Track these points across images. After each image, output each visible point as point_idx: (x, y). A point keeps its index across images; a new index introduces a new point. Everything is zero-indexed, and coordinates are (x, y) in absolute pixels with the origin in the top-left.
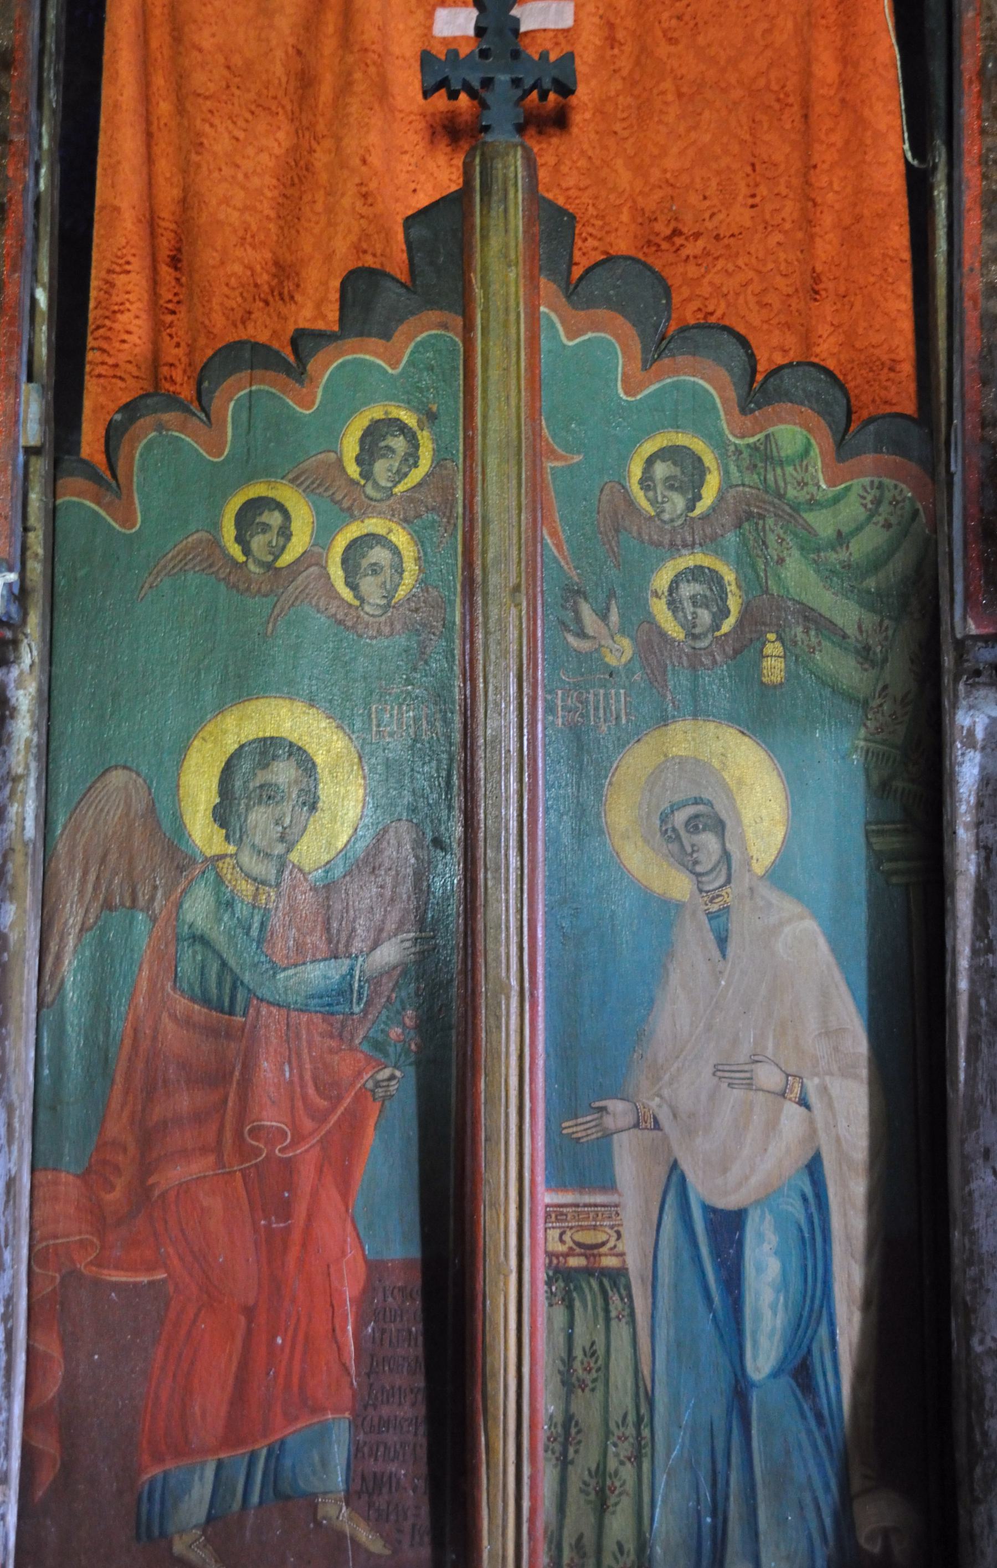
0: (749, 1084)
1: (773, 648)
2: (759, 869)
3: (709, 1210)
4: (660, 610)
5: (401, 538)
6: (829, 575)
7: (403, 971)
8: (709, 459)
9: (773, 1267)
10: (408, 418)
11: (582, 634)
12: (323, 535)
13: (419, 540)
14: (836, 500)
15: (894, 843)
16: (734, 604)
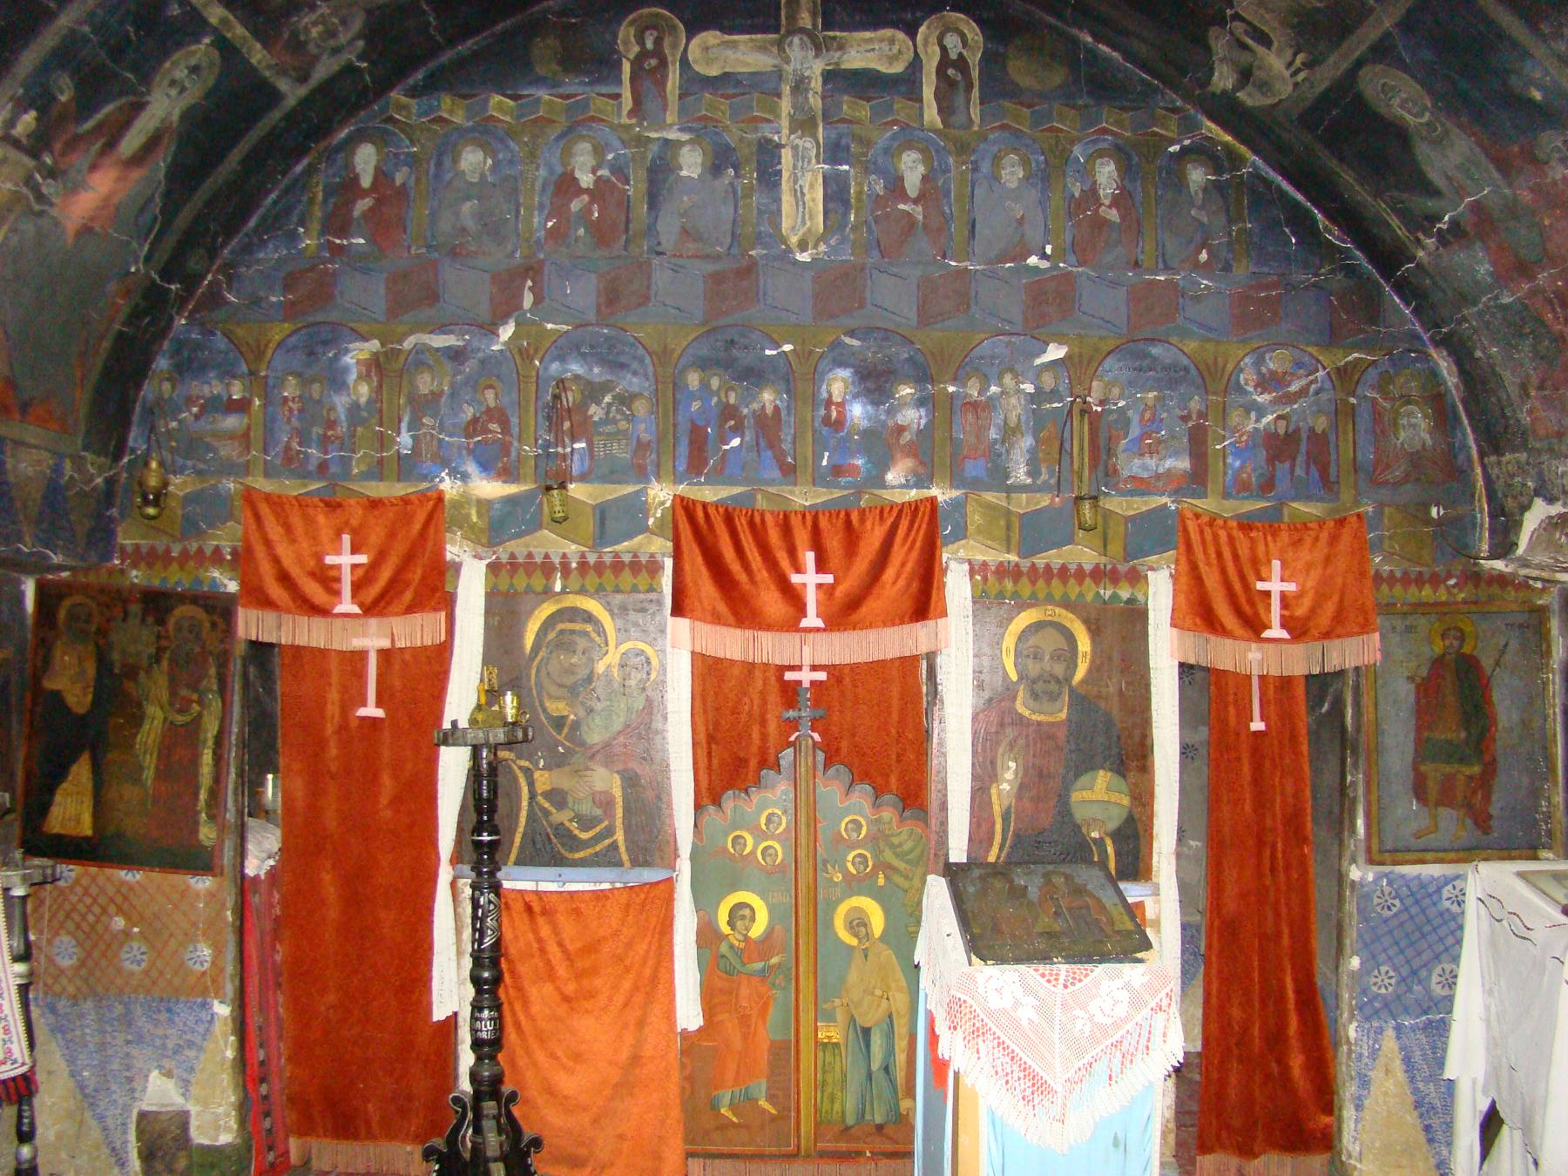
0: (873, 994)
2: (877, 936)
5: (777, 846)
8: (863, 823)
10: (780, 813)
16: (870, 864)
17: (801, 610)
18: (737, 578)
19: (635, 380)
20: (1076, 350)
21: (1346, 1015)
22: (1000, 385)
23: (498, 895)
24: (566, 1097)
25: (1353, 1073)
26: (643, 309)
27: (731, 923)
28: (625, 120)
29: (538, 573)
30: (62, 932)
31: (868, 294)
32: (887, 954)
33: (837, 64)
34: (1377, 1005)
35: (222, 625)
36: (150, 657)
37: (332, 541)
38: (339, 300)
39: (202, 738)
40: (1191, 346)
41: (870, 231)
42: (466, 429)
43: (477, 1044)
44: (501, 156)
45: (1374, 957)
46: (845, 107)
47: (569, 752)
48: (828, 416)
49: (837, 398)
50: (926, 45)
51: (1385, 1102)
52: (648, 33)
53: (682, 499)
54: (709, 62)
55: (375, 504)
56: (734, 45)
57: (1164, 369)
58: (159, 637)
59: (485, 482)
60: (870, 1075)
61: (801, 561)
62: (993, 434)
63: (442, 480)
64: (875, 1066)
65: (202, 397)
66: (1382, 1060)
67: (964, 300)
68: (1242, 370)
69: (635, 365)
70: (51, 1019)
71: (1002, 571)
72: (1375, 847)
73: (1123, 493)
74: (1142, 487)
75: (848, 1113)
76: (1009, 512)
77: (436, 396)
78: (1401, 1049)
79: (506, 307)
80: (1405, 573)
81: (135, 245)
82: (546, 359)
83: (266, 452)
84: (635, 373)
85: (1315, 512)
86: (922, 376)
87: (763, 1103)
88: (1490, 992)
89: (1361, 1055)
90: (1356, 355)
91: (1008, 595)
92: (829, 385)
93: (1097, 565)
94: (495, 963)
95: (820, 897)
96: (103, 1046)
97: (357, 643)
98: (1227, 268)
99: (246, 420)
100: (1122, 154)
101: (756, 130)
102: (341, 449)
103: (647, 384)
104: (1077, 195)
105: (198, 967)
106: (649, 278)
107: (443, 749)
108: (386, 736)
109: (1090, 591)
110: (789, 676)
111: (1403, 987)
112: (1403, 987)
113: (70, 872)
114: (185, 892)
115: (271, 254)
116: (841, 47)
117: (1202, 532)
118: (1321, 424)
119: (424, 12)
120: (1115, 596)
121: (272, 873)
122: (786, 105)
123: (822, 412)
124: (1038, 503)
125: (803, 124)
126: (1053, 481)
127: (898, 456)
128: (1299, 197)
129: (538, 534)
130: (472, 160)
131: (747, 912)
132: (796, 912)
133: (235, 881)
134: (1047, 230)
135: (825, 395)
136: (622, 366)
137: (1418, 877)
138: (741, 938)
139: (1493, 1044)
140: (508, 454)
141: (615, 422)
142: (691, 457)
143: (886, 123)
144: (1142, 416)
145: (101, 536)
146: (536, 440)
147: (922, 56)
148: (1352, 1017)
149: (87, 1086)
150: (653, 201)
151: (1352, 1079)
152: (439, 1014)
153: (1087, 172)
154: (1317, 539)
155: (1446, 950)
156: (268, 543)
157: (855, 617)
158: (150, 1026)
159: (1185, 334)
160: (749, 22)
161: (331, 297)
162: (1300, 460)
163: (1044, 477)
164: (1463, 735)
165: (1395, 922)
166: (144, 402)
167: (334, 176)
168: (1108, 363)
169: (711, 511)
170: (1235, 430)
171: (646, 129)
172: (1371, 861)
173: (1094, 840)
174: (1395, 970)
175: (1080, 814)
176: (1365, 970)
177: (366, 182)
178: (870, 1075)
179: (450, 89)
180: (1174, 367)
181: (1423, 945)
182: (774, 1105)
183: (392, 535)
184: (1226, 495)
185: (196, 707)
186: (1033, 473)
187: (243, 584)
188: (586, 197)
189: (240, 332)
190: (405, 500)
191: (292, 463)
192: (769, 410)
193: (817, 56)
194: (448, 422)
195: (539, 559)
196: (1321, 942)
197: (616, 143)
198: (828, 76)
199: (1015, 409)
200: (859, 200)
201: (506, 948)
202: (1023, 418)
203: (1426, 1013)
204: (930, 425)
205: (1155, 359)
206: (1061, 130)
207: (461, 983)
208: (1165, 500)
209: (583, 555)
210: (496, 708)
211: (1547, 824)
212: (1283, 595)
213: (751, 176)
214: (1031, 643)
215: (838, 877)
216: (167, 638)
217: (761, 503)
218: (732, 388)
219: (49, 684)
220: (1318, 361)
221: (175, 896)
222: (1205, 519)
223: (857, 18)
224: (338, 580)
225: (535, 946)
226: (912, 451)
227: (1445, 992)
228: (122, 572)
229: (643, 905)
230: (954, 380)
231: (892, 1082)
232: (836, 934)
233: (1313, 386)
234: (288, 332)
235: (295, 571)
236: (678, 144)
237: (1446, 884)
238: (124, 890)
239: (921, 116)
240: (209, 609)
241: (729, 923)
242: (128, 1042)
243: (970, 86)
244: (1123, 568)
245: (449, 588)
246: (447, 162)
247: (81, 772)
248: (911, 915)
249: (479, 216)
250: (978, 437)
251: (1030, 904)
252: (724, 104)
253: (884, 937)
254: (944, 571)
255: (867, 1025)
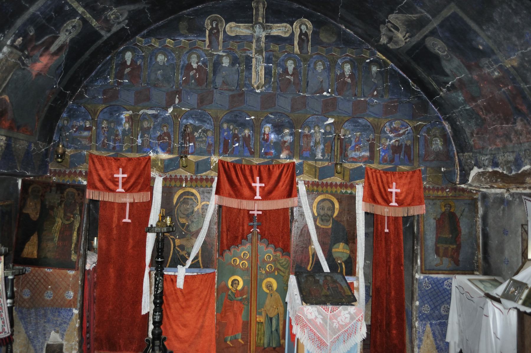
0: (273, 307)
1: (276, 272)
3: (270, 318)
4: (267, 269)
5: (246, 262)
12: (240, 262)
13: (248, 262)
16: (273, 268)
17: (255, 194)
18: (237, 184)
19: (208, 126)
20: (337, 120)
21: (415, 319)
22: (314, 130)
23: (163, 277)
24: (181, 338)
25: (417, 337)
26: (211, 105)
27: (232, 285)
28: (207, 48)
29: (178, 181)
30: (26, 287)
31: (276, 103)
32: (277, 295)
33: (269, 34)
34: (424, 316)
35: (81, 195)
36: (58, 203)
37: (116, 170)
38: (120, 99)
39: (74, 228)
40: (371, 119)
41: (278, 84)
42: (158, 138)
43: (154, 323)
44: (169, 57)
45: (423, 302)
46: (271, 46)
47: (186, 234)
48: (264, 137)
49: (267, 133)
50: (296, 28)
51: (427, 347)
52: (214, 22)
53: (221, 161)
54: (232, 32)
55: (130, 159)
56: (239, 27)
57: (363, 126)
58: (61, 197)
59: (163, 154)
60: (272, 332)
61: (255, 179)
62: (312, 144)
63: (150, 153)
64: (273, 329)
65: (77, 126)
66: (426, 334)
67: (305, 105)
68: (385, 127)
69: (208, 121)
70: (20, 315)
71: (313, 184)
72: (423, 269)
73: (349, 162)
74: (355, 160)
75: (265, 344)
76: (316, 167)
77: (149, 128)
78: (432, 330)
79: (171, 103)
80: (433, 187)
81: (55, 79)
82: (182, 119)
83: (96, 143)
84: (208, 124)
85: (406, 168)
86: (291, 126)
87: (240, 340)
88: (460, 316)
89: (419, 332)
90: (420, 123)
91: (315, 191)
92: (265, 129)
93: (341, 183)
94: (161, 298)
95: (258, 278)
96: (36, 324)
97: (123, 200)
98: (382, 96)
99: (90, 133)
100: (351, 62)
101: (245, 53)
102: (120, 143)
103: (211, 127)
104: (338, 74)
105: (69, 298)
106: (213, 95)
107: (148, 233)
108: (131, 228)
109: (339, 190)
110: (251, 212)
111: (432, 311)
112: (432, 311)
113: (29, 269)
114: (66, 275)
115: (99, 83)
116: (271, 29)
117: (372, 174)
118: (409, 143)
119: (146, 13)
120: (346, 192)
121: (94, 268)
122: (254, 45)
123: (262, 136)
124: (324, 164)
125: (259, 51)
126: (329, 158)
127: (284, 150)
128: (405, 76)
129: (178, 170)
130: (161, 58)
131: (237, 282)
132: (251, 283)
133: (82, 272)
134: (329, 85)
135: (263, 132)
136: (205, 121)
137: (437, 278)
138: (235, 290)
139: (461, 332)
140: (170, 146)
141: (202, 137)
142: (224, 149)
143: (283, 52)
144: (356, 139)
145: (44, 166)
146: (179, 142)
147: (294, 32)
148: (416, 320)
149: (31, 336)
150: (215, 72)
151: (417, 339)
152: (144, 312)
153: (342, 68)
154: (407, 177)
155: (446, 300)
156: (97, 170)
157: (270, 196)
158: (52, 317)
159: (369, 116)
160: (244, 20)
161: (118, 97)
162: (402, 153)
163: (326, 157)
164: (451, 236)
165: (429, 292)
166: (58, 126)
167: (119, 61)
168: (346, 124)
169: (229, 164)
170: (383, 144)
171: (213, 51)
172: (422, 273)
173: (339, 263)
174: (430, 306)
175: (335, 255)
176: (421, 306)
177: (129, 63)
178: (272, 332)
179: (154, 36)
180: (365, 125)
181: (438, 298)
182: (243, 341)
183: (134, 169)
184: (380, 163)
185: (73, 219)
186: (323, 155)
187: (88, 182)
188: (195, 71)
189: (89, 107)
190: (139, 159)
191: (105, 147)
192: (247, 136)
193: (263, 31)
194: (152, 136)
195: (178, 177)
196: (407, 295)
197: (204, 55)
198: (267, 37)
199: (318, 137)
200: (275, 74)
201: (165, 292)
202: (321, 140)
203: (439, 319)
204: (294, 141)
205: (360, 123)
206: (334, 55)
207: (150, 303)
208: (361, 164)
209: (192, 176)
210: (164, 221)
211: (477, 264)
212: (396, 193)
213: (243, 67)
214: (321, 205)
215: (264, 272)
216: (64, 198)
217: (244, 162)
218: (236, 129)
219: (25, 211)
220: (409, 124)
221: (63, 276)
222: (374, 170)
223: (276, 20)
224: (118, 182)
225: (174, 291)
226: (288, 148)
227: (445, 313)
228: (50, 177)
229: (206, 279)
230: (301, 128)
231: (278, 334)
232: (263, 289)
233: (407, 132)
234: (104, 107)
235: (105, 179)
236: (222, 56)
237: (445, 280)
238: (46, 275)
239: (294, 49)
240: (78, 190)
241: (231, 285)
242: (45, 322)
243: (308, 41)
244: (349, 184)
245: (151, 185)
246: (153, 58)
247: (34, 238)
248: (285, 284)
249: (162, 75)
250: (307, 145)
251: (320, 285)
252: (236, 45)
253: (277, 290)
254: (297, 184)
255: (271, 317)
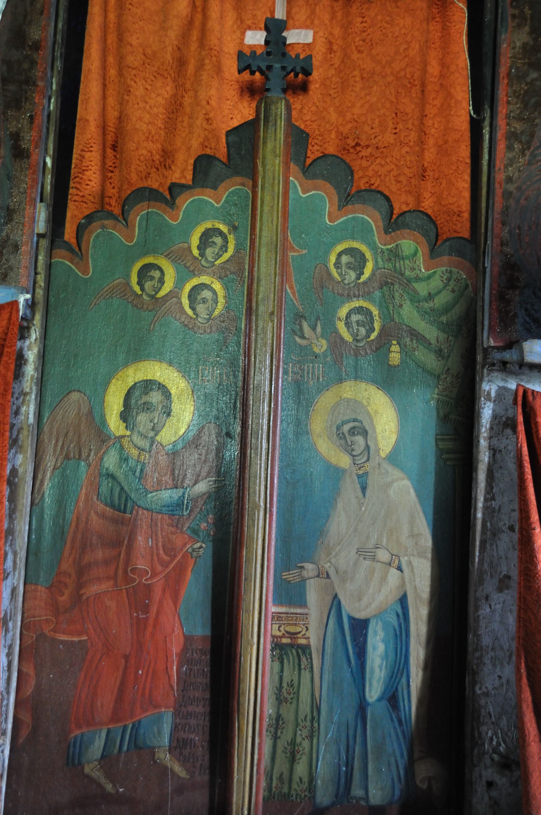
0: (374, 558)
1: (395, 348)
2: (383, 454)
3: (351, 619)
5: (217, 286)
6: (424, 314)
7: (208, 496)
9: (381, 648)
10: (224, 228)
11: (303, 337)
12: (180, 283)
13: (226, 287)
14: (429, 277)
15: (450, 445)
16: (377, 326)
27: (125, 416)
255: (361, 615)
